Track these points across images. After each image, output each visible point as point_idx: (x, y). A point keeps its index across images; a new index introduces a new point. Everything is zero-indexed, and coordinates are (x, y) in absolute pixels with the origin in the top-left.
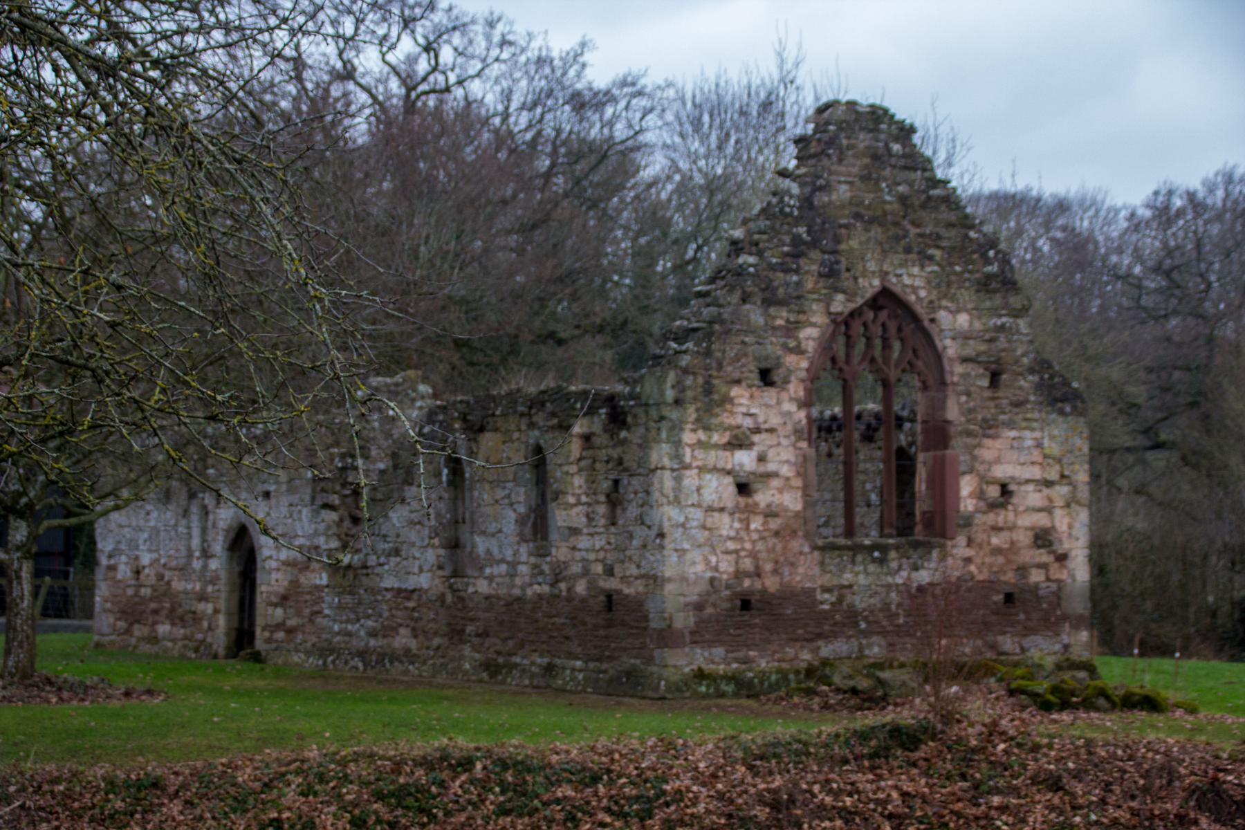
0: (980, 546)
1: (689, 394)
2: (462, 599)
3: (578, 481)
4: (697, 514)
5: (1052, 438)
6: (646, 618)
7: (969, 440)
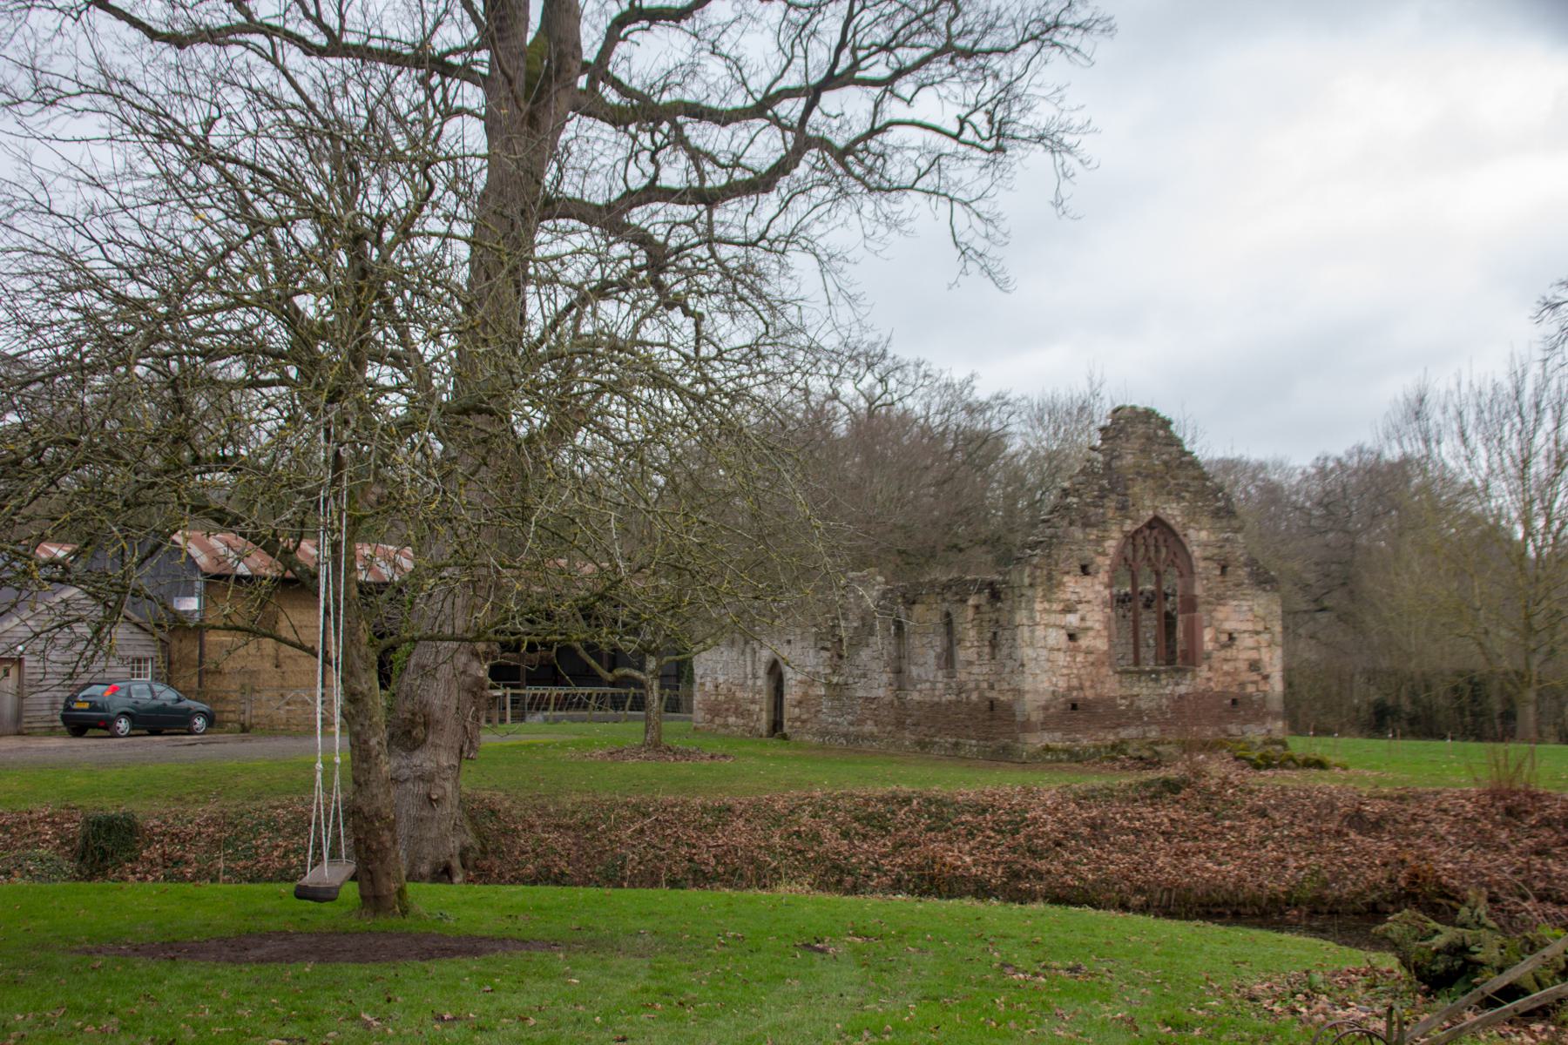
0: (1217, 671)
1: (1039, 580)
3: (972, 633)
4: (1044, 653)
5: (1259, 605)
6: (1014, 715)
7: (1209, 607)
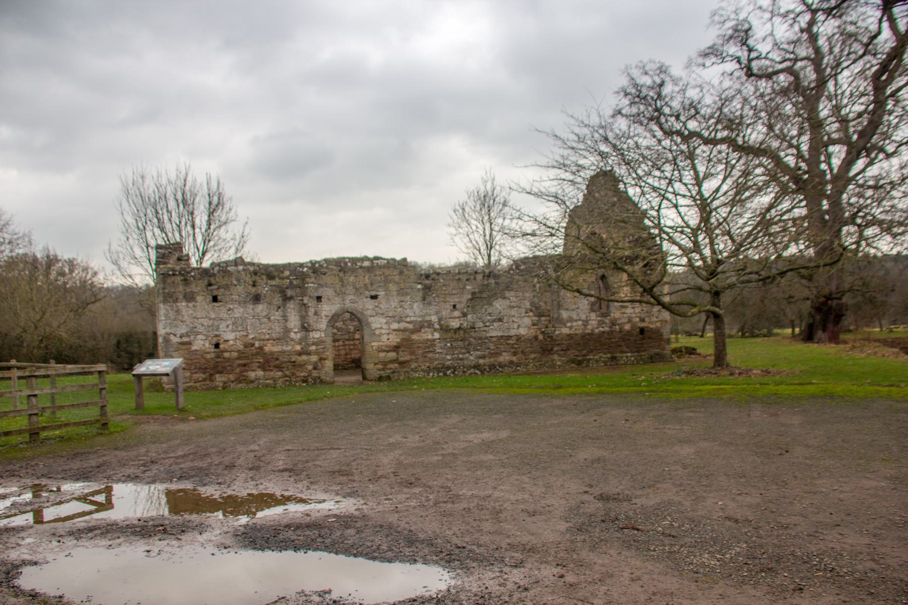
6: (661, 335)
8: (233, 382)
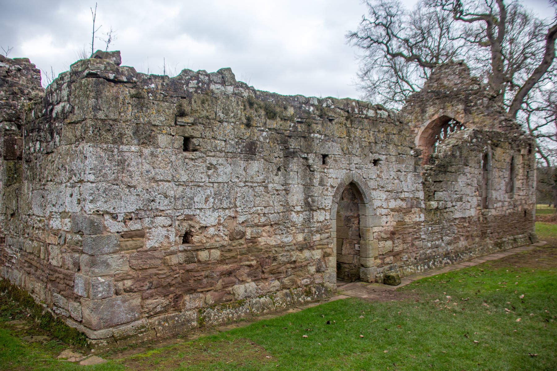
2: (486, 218)
3: (521, 171)
8: (212, 307)
